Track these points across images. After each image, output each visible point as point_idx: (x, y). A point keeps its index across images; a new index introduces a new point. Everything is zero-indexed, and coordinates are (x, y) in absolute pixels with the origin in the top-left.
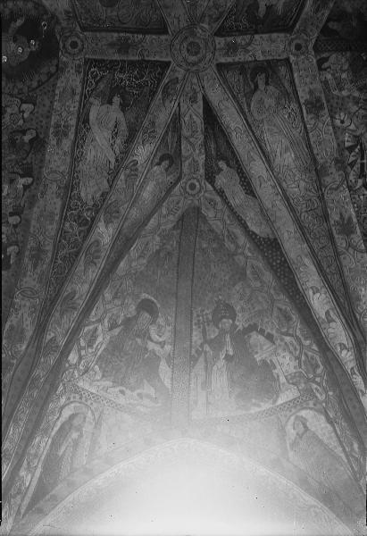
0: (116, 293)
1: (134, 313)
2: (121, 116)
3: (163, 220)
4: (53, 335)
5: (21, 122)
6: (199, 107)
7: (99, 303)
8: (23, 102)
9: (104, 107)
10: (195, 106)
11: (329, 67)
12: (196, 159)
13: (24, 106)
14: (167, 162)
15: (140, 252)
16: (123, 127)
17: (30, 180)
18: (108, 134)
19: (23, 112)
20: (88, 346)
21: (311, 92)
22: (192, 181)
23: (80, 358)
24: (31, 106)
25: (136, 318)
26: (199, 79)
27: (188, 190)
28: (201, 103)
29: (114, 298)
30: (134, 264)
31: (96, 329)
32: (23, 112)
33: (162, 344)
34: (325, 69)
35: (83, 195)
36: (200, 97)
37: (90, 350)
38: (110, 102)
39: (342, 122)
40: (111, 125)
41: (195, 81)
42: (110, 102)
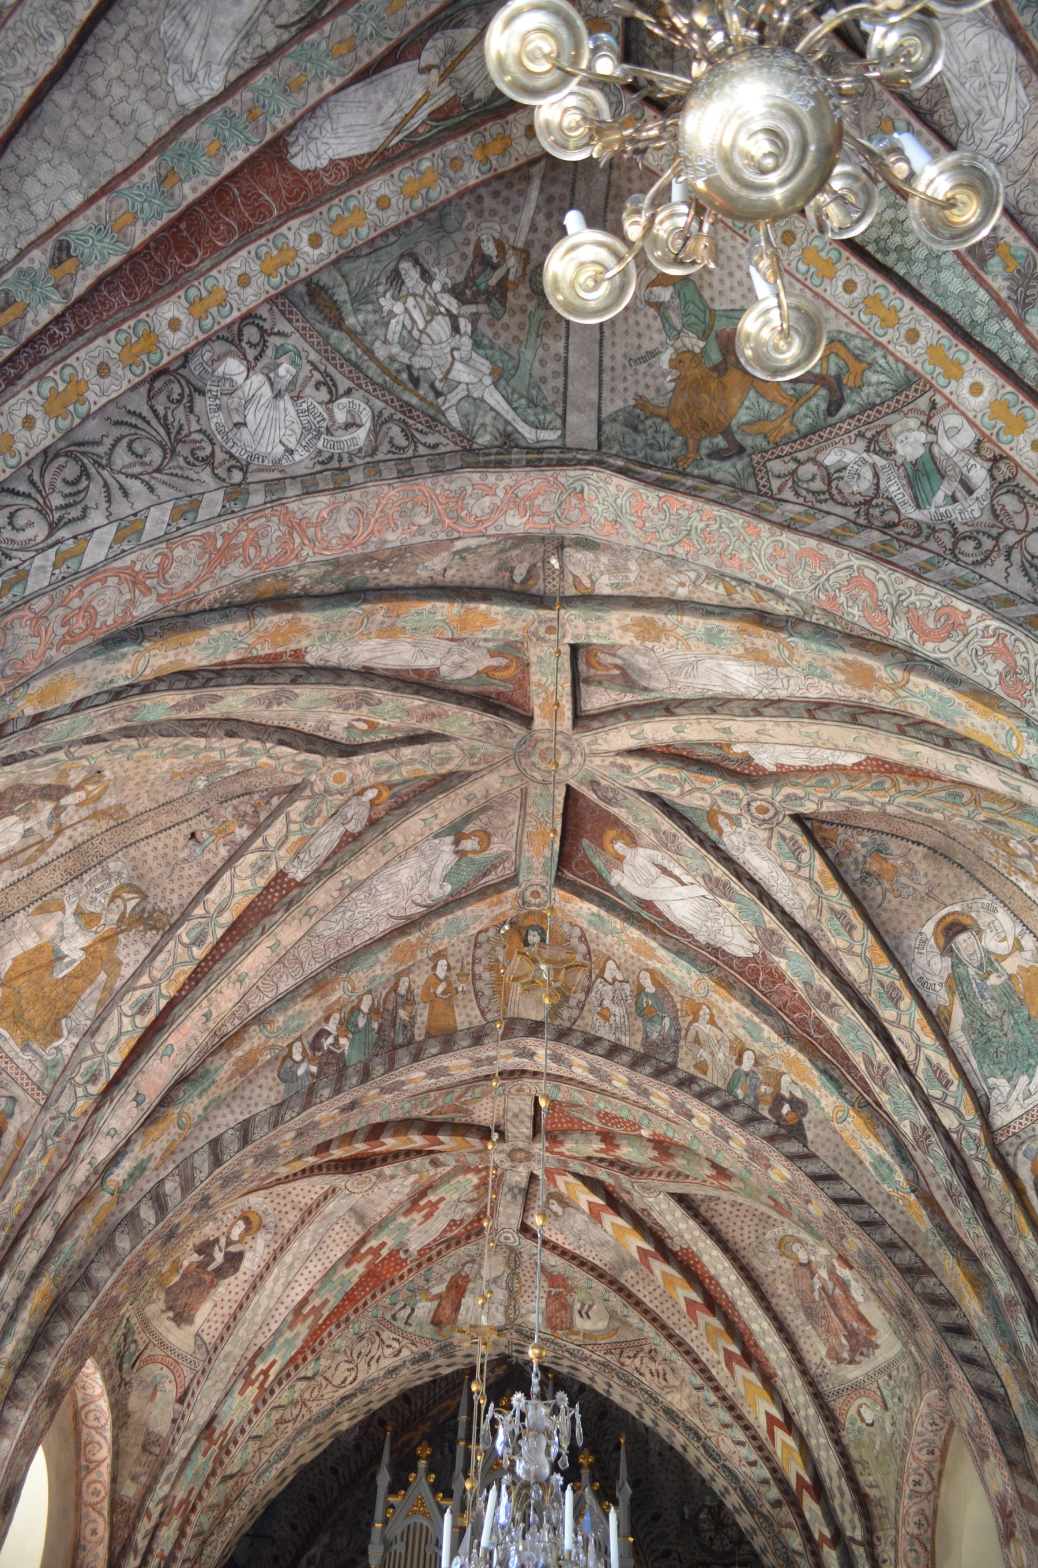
0: (892, 999)
1: (948, 961)
2: (641, 851)
3: (805, 872)
4: (907, 1122)
5: (627, 986)
6: (638, 765)
7: (895, 1033)
8: (601, 975)
9: (626, 868)
10: (635, 770)
11: (590, 577)
12: (718, 790)
13: (607, 975)
14: (721, 818)
15: (842, 930)
16: (659, 856)
17: (705, 1010)
18: (666, 881)
19: (614, 980)
20: (946, 1086)
21: (625, 628)
22: (753, 810)
23: (956, 1110)
24: (611, 965)
25: (957, 962)
26: (594, 754)
27: (767, 816)
28: (631, 762)
29: (896, 1005)
30: (857, 949)
31: (928, 1060)
32: (614, 980)
33: (1018, 947)
34: (593, 583)
35: (741, 954)
36: (620, 760)
37: (953, 1088)
38: (620, 858)
39: (682, 585)
40: (654, 871)
41: (597, 761)
42: (620, 858)
